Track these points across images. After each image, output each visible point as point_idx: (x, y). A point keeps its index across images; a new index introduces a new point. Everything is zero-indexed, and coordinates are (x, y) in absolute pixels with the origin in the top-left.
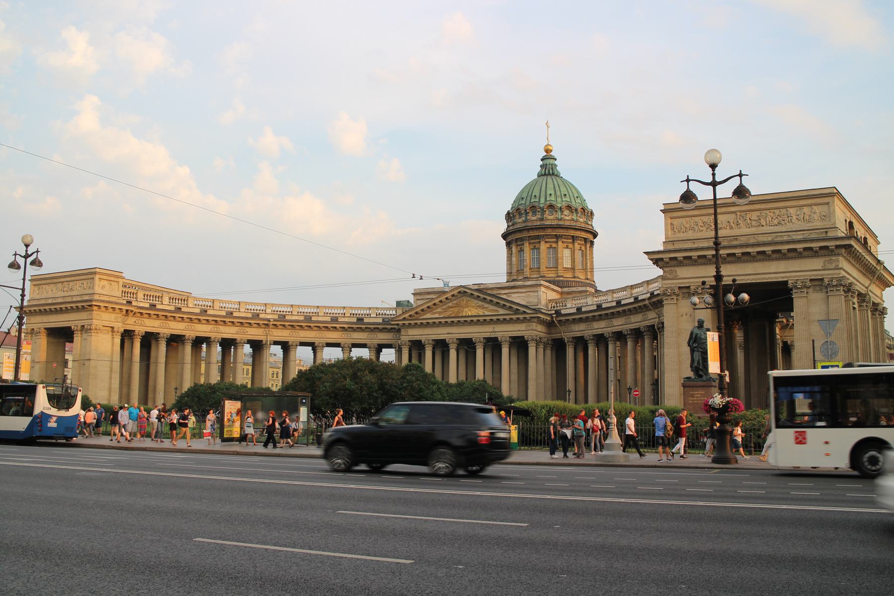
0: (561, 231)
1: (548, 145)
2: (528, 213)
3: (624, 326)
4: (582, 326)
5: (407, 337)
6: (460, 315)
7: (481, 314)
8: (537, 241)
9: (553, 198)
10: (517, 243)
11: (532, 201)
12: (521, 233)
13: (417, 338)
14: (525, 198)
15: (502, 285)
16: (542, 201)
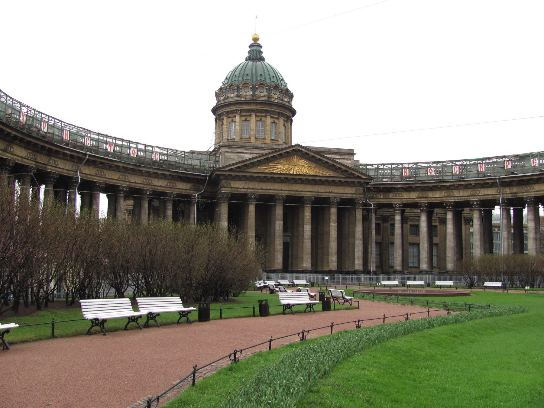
0: (282, 109)
1: (256, 34)
2: (257, 88)
3: (444, 198)
4: (391, 196)
5: (229, 189)
6: (291, 172)
7: (311, 173)
8: (262, 114)
9: (276, 81)
10: (241, 114)
11: (259, 79)
12: (248, 105)
13: (241, 191)
14: (250, 74)
15: (317, 149)
16: (268, 81)
